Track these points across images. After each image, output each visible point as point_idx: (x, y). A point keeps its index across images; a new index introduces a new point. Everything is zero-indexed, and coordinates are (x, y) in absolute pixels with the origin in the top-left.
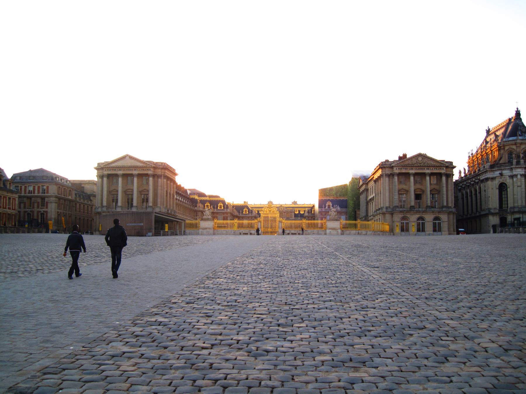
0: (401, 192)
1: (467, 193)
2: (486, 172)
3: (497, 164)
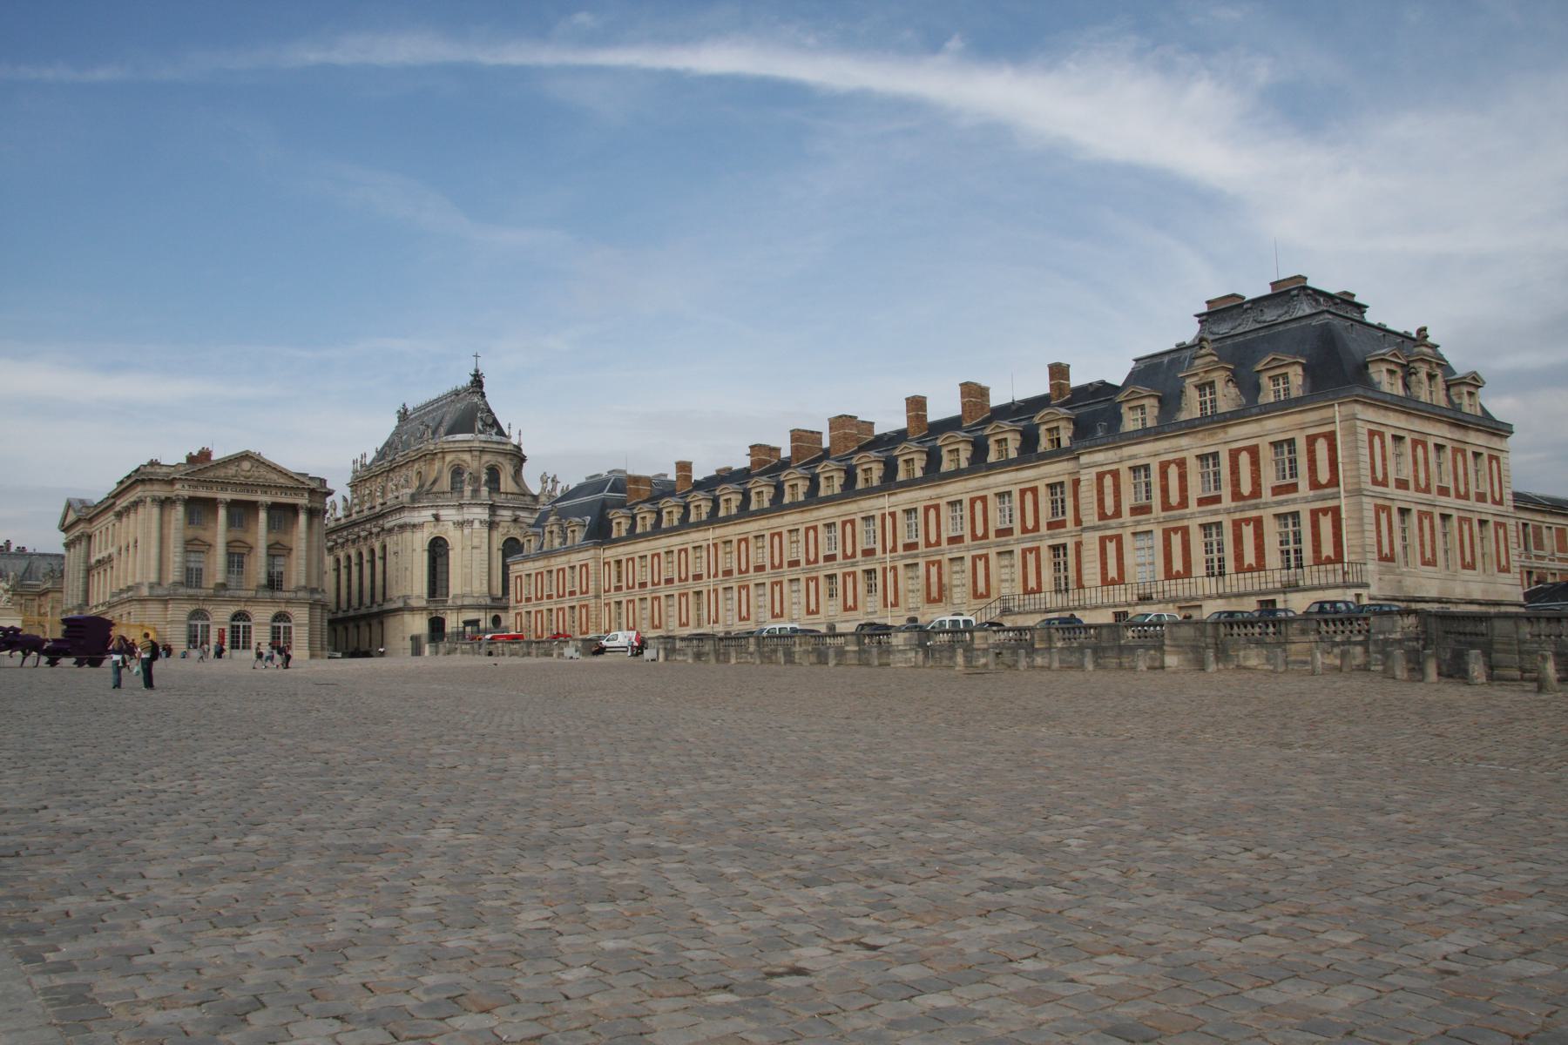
0: (193, 546)
1: (349, 557)
2: (402, 509)
3: (428, 492)
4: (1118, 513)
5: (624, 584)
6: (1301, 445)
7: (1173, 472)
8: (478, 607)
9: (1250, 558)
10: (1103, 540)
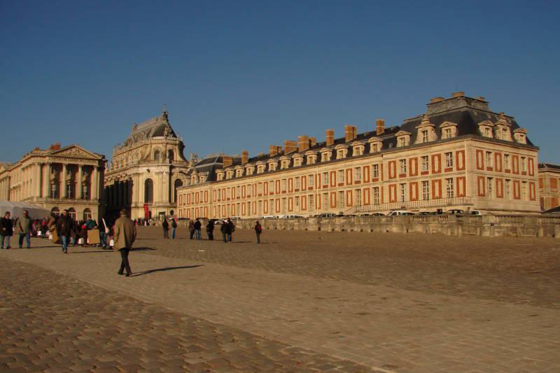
4: (395, 177)
5: (221, 198)
6: (454, 154)
7: (413, 162)
8: (164, 207)
9: (437, 194)
10: (390, 186)
